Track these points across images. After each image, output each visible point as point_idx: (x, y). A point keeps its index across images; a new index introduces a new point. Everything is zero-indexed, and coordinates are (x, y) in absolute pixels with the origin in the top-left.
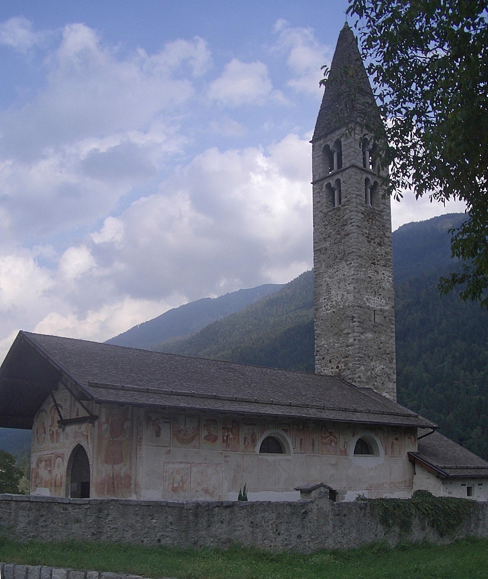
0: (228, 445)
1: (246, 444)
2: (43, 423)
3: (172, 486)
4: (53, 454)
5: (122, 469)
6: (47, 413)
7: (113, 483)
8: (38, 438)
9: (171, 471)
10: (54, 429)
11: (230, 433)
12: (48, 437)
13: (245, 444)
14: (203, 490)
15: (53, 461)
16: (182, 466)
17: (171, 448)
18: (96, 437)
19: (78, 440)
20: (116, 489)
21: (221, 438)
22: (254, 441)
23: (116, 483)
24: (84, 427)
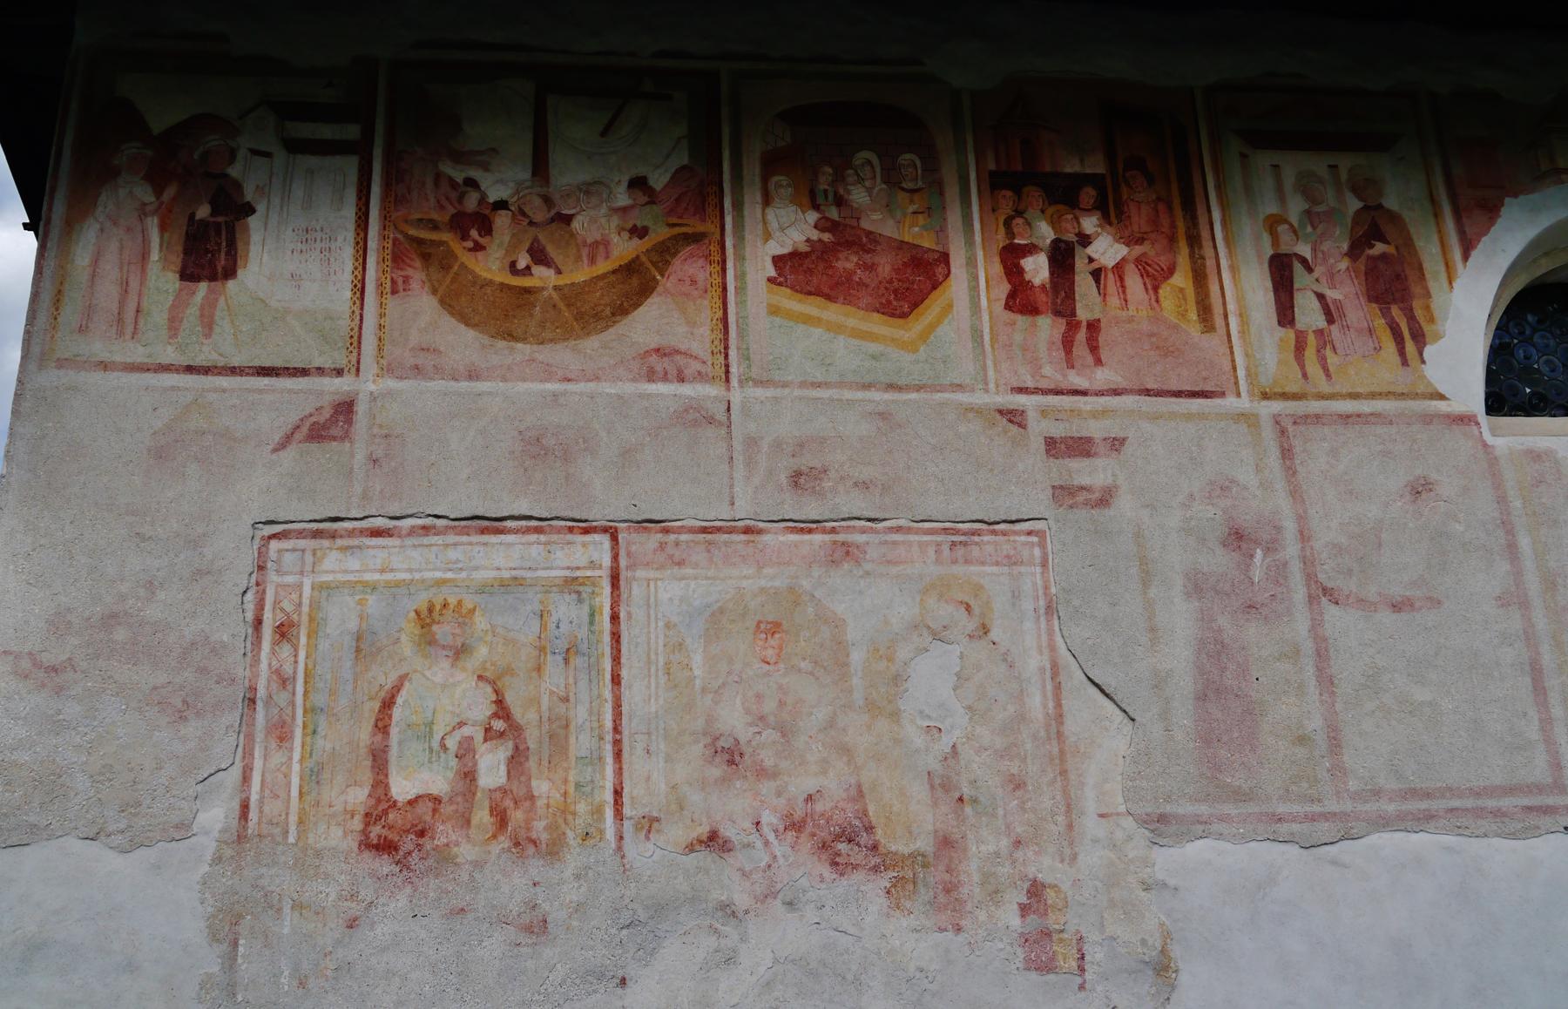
0: (1084, 339)
1: (1309, 314)
3: (359, 796)
9: (341, 617)
11: (1089, 224)
13: (1286, 315)
14: (795, 825)
16: (499, 556)
17: (368, 384)
21: (988, 269)
22: (1395, 290)
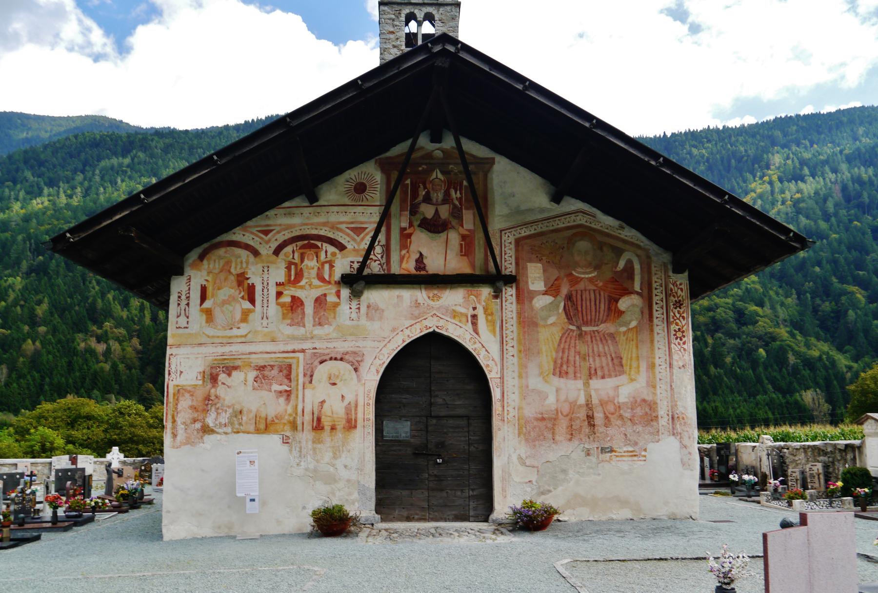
2: (241, 279)
4: (303, 351)
5: (624, 389)
6: (256, 253)
7: (590, 418)
8: (209, 313)
10: (307, 295)
12: (273, 310)
15: (299, 371)
18: (514, 321)
19: (425, 323)
20: (600, 429)
23: (599, 416)
24: (454, 298)
